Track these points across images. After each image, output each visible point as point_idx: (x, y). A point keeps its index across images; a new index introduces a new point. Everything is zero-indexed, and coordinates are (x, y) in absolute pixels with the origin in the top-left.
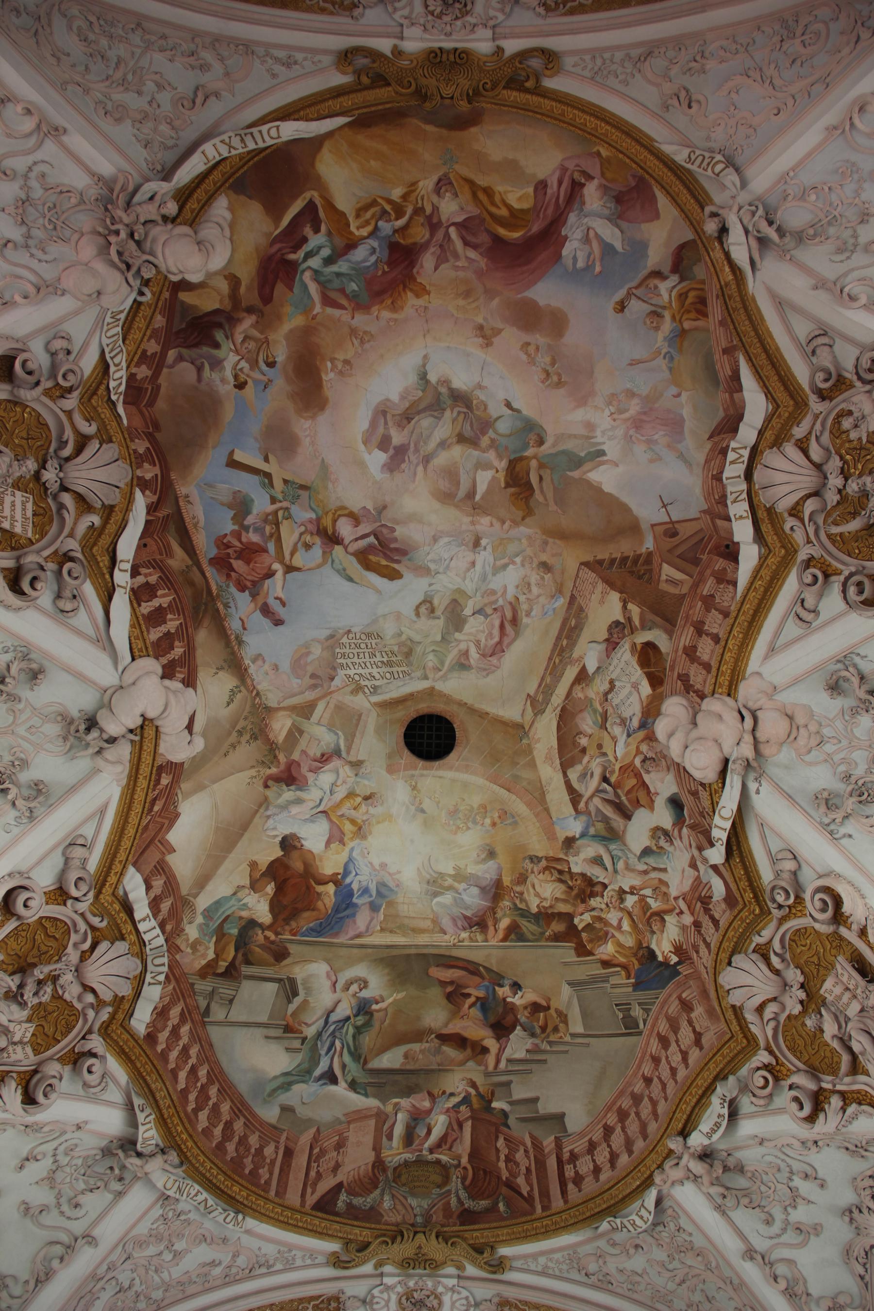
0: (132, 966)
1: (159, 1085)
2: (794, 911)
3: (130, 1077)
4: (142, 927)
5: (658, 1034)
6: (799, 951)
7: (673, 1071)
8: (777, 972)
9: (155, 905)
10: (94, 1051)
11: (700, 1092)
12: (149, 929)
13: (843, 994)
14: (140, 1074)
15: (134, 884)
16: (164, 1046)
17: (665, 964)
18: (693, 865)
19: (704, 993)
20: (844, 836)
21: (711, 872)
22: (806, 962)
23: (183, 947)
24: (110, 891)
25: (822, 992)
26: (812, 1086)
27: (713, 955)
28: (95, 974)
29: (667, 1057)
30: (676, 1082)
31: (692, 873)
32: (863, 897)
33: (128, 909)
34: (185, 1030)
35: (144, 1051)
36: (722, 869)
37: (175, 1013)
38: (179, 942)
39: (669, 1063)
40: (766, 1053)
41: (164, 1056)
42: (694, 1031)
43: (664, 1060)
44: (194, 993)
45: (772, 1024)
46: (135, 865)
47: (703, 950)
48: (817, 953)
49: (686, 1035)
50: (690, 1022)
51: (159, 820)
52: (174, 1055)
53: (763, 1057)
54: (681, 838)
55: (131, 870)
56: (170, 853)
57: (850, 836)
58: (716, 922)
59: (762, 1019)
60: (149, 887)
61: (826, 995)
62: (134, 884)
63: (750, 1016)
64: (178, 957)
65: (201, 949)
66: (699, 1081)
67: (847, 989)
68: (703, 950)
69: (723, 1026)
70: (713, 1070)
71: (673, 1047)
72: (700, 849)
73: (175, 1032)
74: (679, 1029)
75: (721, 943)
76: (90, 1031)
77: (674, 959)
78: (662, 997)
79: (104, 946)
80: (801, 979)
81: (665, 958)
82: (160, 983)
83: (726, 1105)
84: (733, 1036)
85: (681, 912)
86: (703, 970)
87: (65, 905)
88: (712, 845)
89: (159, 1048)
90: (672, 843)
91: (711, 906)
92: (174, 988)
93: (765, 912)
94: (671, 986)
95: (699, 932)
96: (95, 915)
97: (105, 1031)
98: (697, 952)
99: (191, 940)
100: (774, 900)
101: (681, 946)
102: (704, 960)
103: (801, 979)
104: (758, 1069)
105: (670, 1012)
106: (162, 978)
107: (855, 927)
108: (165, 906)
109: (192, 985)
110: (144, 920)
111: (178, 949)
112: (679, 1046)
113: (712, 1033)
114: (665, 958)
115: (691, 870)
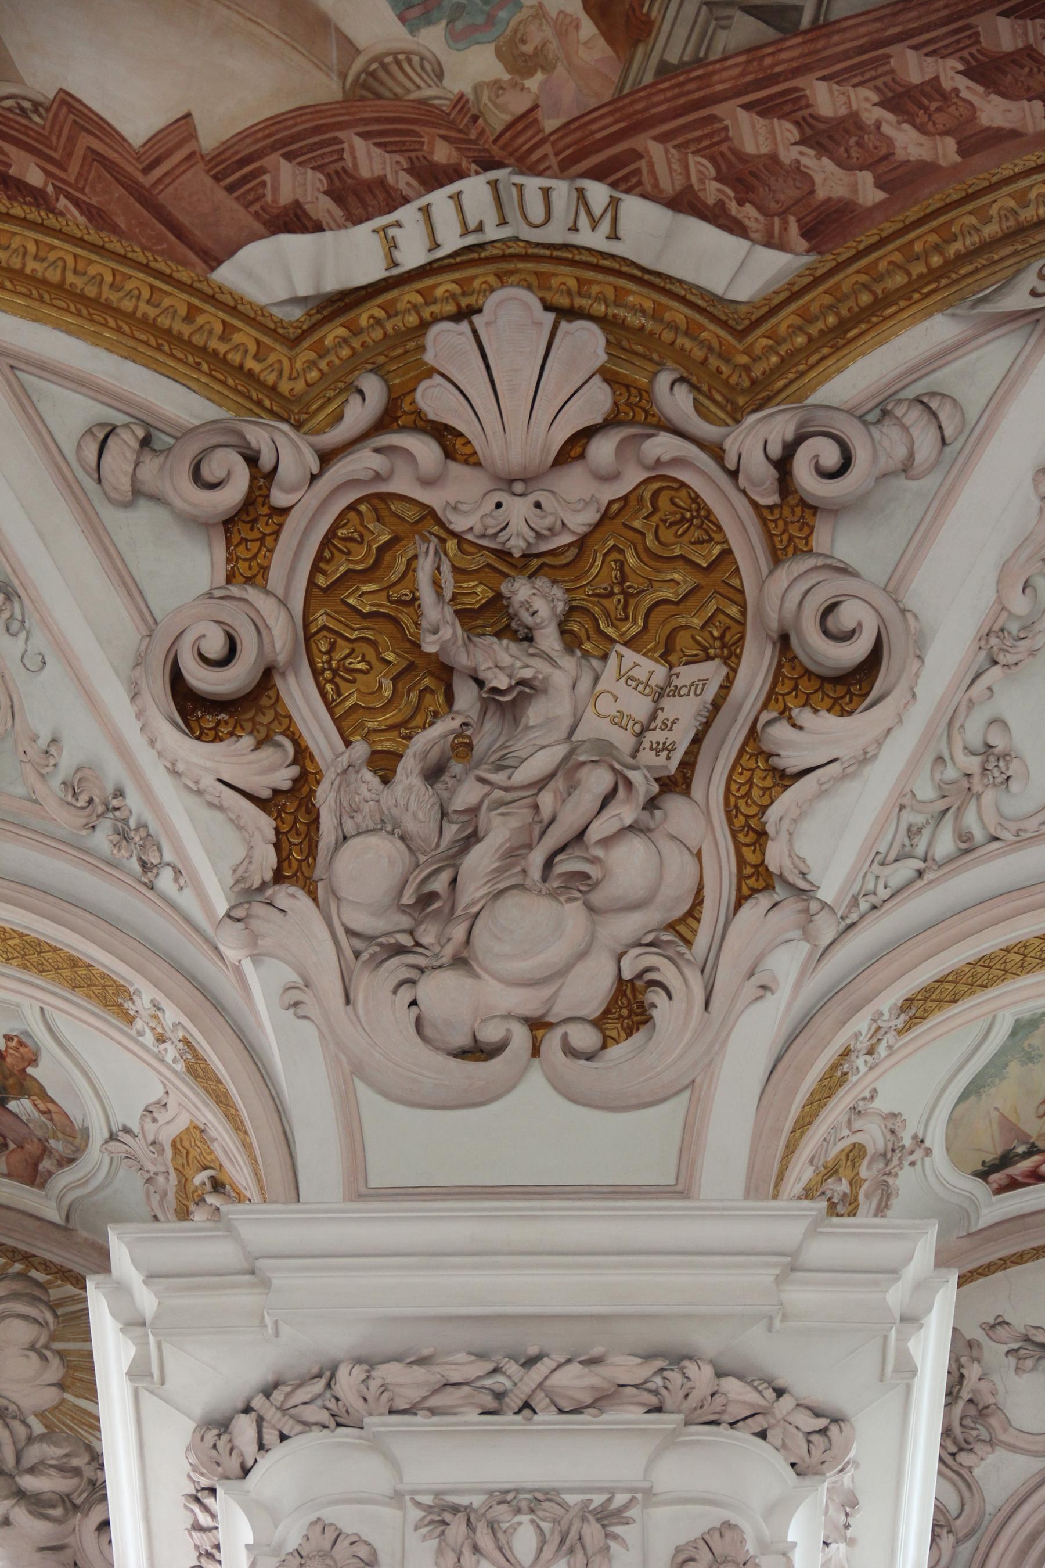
0: (513, 315)
1: (1003, 201)
3: (942, 307)
4: (413, 255)
9: (362, 200)
10: (776, 450)
12: (425, 228)
14: (934, 275)
15: (275, 271)
16: (866, 178)
23: (519, 104)
24: (279, 353)
28: (516, 436)
33: (343, 303)
34: (825, 99)
35: (860, 255)
37: (752, 134)
38: (498, 120)
41: (901, 179)
44: (698, 62)
46: (213, 261)
51: (74, 168)
52: (909, 143)
55: (227, 274)
56: (193, 136)
60: (295, 220)
62: (275, 271)
64: (550, 125)
65: (537, 36)
73: (824, 136)
76: (716, 451)
79: (434, 400)
82: (614, 203)
87: (285, 511)
89: (868, 191)
92: (658, 139)
96: (339, 417)
97: (736, 397)
99: (499, 72)
106: (598, 193)
108: (368, 160)
109: (664, 70)
110: (392, 245)
111: (527, 119)
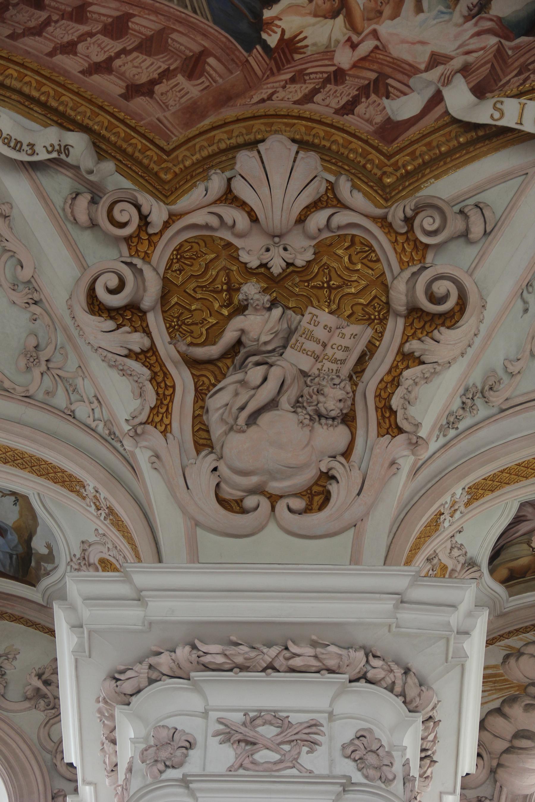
2: (401, 239)
5: (128, 16)
6: (340, 252)
7: (69, 48)
8: (301, 220)
11: (54, 104)
13: (318, 341)
17: (260, 25)
18: (436, 60)
19: (225, 98)
20: (525, 302)
21: (429, 92)
22: (326, 266)
25: (310, 309)
26: (147, 302)
27: (296, 110)
29: (91, 35)
30: (51, 54)
31: (422, 60)
32: (462, 354)
36: (438, 111)
39: (82, 38)
40: (165, 217)
42: (153, 83)
43: (84, 28)
45: (214, 221)
47: (298, 91)
48: (347, 283)
49: (142, 67)
50: (166, 74)
53: (158, 213)
54: (478, 34)
57: (526, 311)
58: (349, 108)
59: (215, 203)
61: (307, 317)
63: (216, 183)
66: (67, 97)
67: (325, 345)
68: (298, 91)
69: (179, 135)
70: (100, 122)
71: (116, 46)
72: (465, 70)
74: (149, 54)
75: (320, 122)
77: (272, 40)
78: (196, 19)
80: (300, 262)
81: (270, 23)
83: (54, 155)
84: (168, 153)
85: (354, 46)
86: (264, 93)
88: (480, 91)
90: (467, 18)
91: (373, 97)
93: (387, 195)
94: (223, 36)
95: (327, 81)
98: (293, 80)
100: (418, 210)
101: (297, 50)
102: (281, 94)
103: (300, 262)
104: (138, 207)
105: (174, 36)
107: (414, 345)
112: (118, 55)
113: (160, 115)
114: (270, 23)
115: (426, 57)
